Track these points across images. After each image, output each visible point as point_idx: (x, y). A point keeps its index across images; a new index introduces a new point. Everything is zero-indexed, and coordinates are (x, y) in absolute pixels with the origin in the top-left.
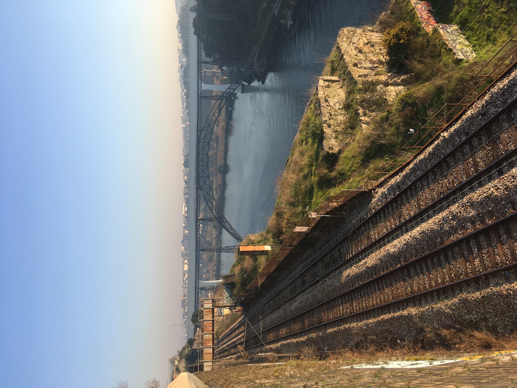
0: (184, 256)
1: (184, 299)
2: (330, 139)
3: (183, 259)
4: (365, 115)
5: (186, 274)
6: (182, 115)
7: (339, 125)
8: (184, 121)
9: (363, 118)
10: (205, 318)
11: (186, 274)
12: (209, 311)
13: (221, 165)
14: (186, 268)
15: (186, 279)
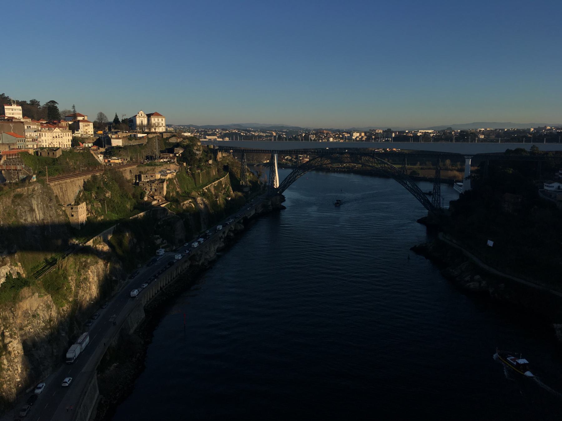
0: (370, 134)
1: (324, 133)
3: (368, 130)
5: (349, 135)
6: (548, 128)
8: (538, 130)
10: (12, 166)
11: (349, 135)
12: (15, 168)
13: (419, 174)
14: (356, 135)
15: (344, 134)
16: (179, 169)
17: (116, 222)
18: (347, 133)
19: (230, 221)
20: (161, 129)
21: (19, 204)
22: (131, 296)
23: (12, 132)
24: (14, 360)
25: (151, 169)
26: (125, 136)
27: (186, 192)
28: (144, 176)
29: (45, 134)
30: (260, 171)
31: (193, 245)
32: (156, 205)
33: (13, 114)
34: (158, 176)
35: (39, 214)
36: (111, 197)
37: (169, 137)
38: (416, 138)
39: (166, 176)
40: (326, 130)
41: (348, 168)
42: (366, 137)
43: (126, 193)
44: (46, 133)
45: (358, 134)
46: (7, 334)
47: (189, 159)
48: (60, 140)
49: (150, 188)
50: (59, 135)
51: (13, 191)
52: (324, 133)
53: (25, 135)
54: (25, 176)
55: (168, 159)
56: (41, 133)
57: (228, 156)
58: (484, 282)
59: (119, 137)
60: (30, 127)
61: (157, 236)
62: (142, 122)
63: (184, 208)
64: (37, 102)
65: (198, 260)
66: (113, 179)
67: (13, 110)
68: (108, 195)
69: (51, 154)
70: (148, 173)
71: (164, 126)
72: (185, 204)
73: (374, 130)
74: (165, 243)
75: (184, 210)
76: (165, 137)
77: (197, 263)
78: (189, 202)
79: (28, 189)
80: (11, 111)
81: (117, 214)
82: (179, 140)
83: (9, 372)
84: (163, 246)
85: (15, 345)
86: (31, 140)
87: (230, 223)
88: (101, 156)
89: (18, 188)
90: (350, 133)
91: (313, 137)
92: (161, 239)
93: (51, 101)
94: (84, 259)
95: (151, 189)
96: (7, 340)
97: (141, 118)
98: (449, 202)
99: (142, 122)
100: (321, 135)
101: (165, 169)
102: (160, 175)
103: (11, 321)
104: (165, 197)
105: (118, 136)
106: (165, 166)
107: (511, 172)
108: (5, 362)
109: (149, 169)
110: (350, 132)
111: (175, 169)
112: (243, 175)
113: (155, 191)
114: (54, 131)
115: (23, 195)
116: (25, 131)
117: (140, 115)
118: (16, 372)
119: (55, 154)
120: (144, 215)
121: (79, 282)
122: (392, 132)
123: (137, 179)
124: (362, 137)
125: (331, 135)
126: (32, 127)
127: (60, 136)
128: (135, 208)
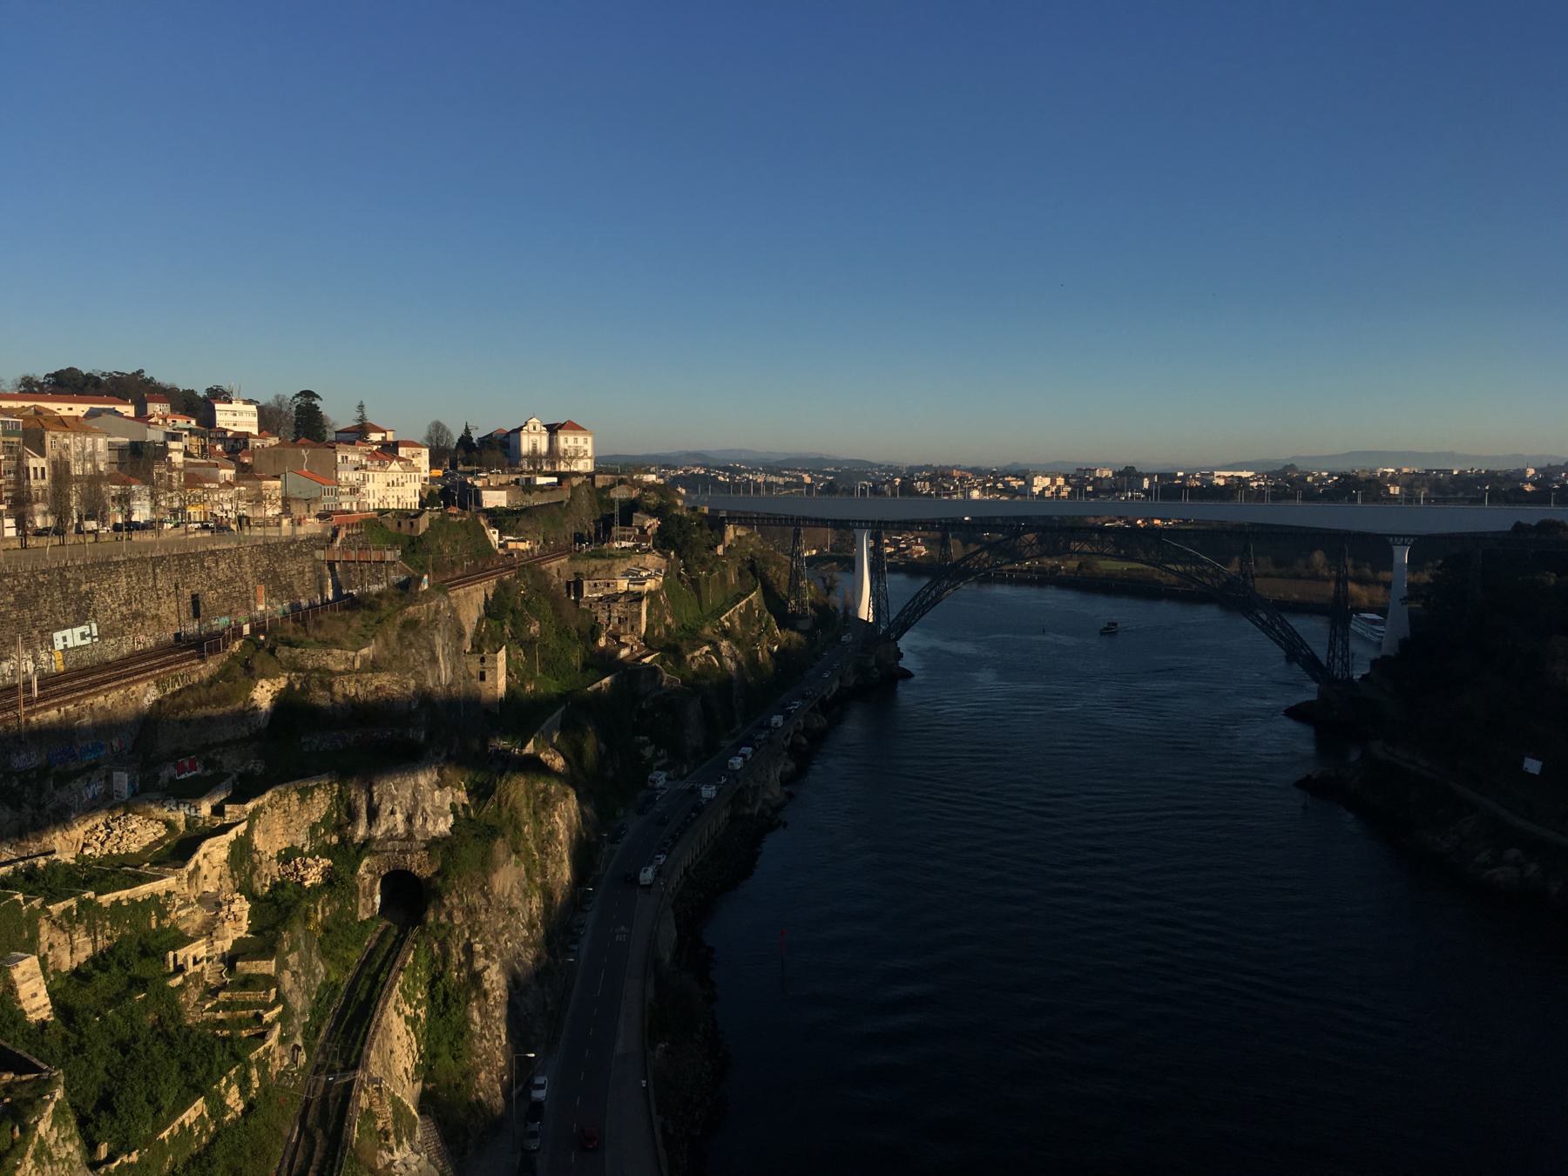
0: (1080, 479)
1: (954, 478)
2: (290, 652)
3: (1071, 472)
4: (299, 678)
5: (1022, 483)
7: (302, 660)
9: (293, 674)
10: (375, 552)
11: (1022, 483)
12: (381, 557)
14: (1040, 483)
15: (1009, 482)
16: (667, 567)
17: (562, 698)
18: (1017, 476)
19: (796, 705)
20: (584, 465)
21: (411, 645)
22: (641, 883)
23: (306, 470)
24: (494, 1014)
25: (603, 567)
26: (503, 482)
27: (687, 628)
28: (590, 585)
29: (373, 476)
30: (831, 577)
31: (732, 764)
32: (629, 659)
33: (235, 425)
34: (623, 585)
35: (446, 668)
36: (541, 635)
37: (608, 484)
38: (1209, 492)
39: (644, 583)
40: (958, 470)
41: (1039, 571)
42: (1069, 489)
43: (566, 627)
44: (376, 474)
45: (1047, 481)
46: (479, 947)
47: (679, 541)
48: (398, 491)
49: (607, 614)
50: (398, 480)
51: (399, 612)
52: (954, 478)
53: (337, 476)
54: (403, 578)
55: (633, 541)
56: (367, 473)
57: (750, 535)
58: (1533, 867)
59: (491, 484)
60: (346, 457)
61: (641, 738)
62: (535, 445)
63: (695, 667)
64: (224, 392)
65: (750, 801)
66: (539, 591)
67: (235, 415)
68: (534, 629)
69: (405, 525)
70: (596, 576)
71: (589, 458)
72: (696, 657)
73: (1089, 469)
74: (663, 757)
75: (695, 673)
76: (599, 484)
77: (747, 811)
78: (704, 653)
79: (428, 607)
80: (230, 418)
81: (557, 680)
82: (635, 493)
83: (484, 1041)
84: (660, 763)
85: (494, 977)
86: (348, 490)
87: (796, 710)
88: (494, 533)
89: (408, 606)
90: (1023, 478)
91: (923, 487)
92: (653, 747)
93: (302, 392)
94: (542, 785)
95: (609, 619)
96: (480, 964)
97: (532, 437)
98: (1369, 663)
99: (535, 445)
100: (945, 482)
101: (635, 566)
102: (628, 581)
103: (483, 917)
104: (645, 639)
105: (489, 483)
106: (636, 559)
107: (1552, 580)
108: (476, 1016)
109: (599, 567)
110: (1026, 475)
111: (656, 566)
112: (794, 588)
113: (619, 622)
114: (389, 469)
115: (420, 621)
116: (339, 468)
117: (531, 428)
118: (497, 1042)
119: (415, 524)
120: (612, 684)
121: (543, 841)
122: (1141, 476)
123: (572, 591)
124: (1059, 489)
125: (973, 483)
126: (350, 458)
127: (401, 481)
128: (586, 666)
